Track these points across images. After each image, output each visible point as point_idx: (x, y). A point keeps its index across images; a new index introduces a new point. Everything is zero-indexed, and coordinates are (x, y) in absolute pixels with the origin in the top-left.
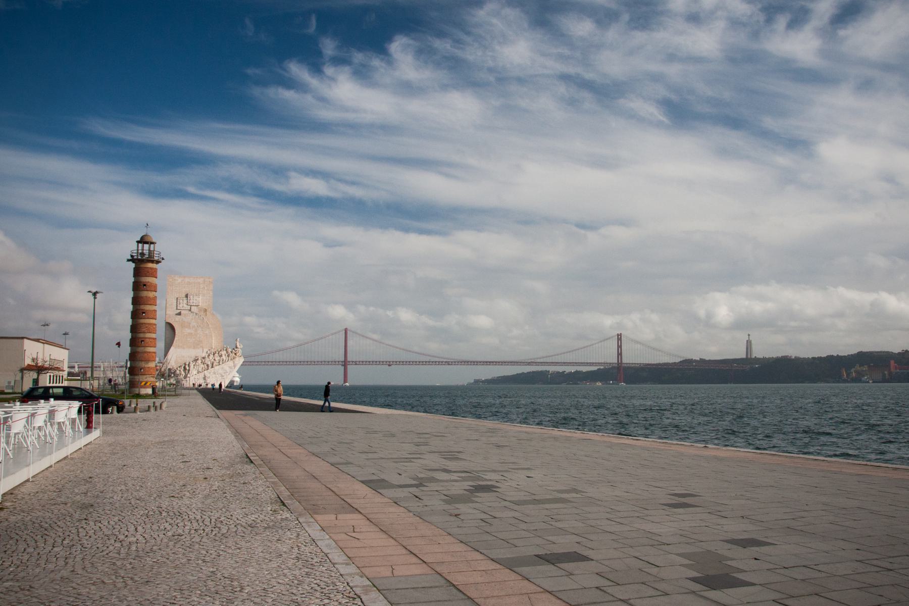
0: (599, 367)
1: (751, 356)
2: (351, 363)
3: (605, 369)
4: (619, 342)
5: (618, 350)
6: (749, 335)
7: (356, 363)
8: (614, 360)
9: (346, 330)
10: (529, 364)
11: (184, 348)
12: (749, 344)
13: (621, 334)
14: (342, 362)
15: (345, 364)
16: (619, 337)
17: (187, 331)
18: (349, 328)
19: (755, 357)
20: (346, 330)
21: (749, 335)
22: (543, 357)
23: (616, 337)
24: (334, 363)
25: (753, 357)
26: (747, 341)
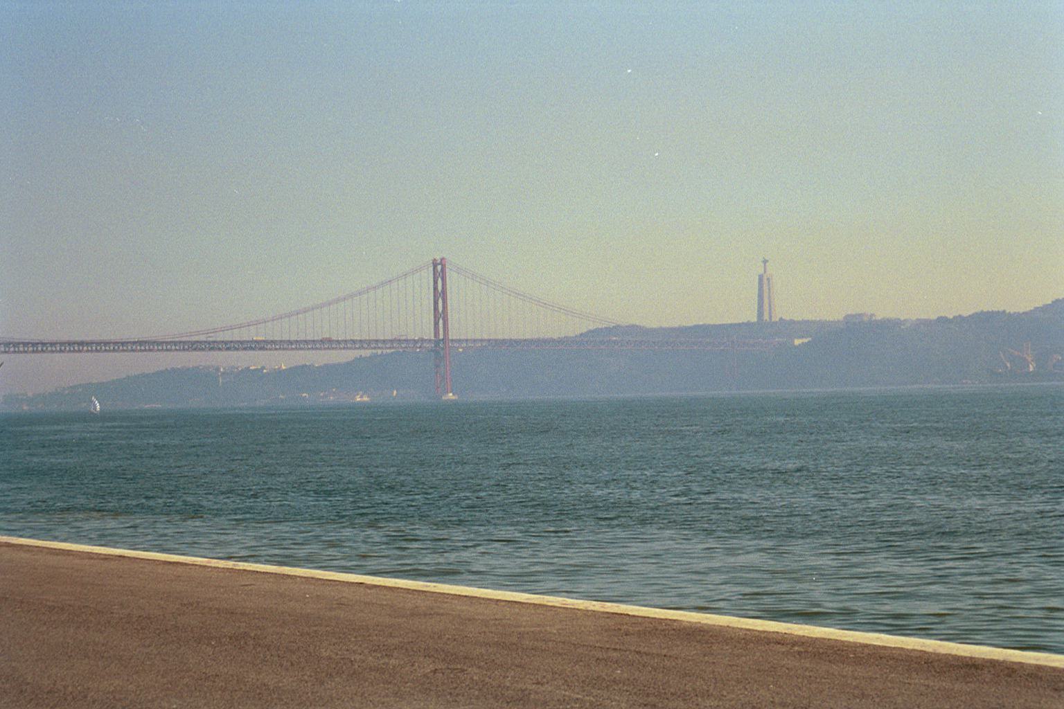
1: (770, 317)
5: (436, 303)
6: (765, 262)
8: (423, 328)
10: (194, 346)
12: (765, 281)
13: (442, 259)
16: (439, 269)
19: (781, 319)
21: (765, 262)
23: (431, 268)
25: (776, 319)
26: (761, 278)
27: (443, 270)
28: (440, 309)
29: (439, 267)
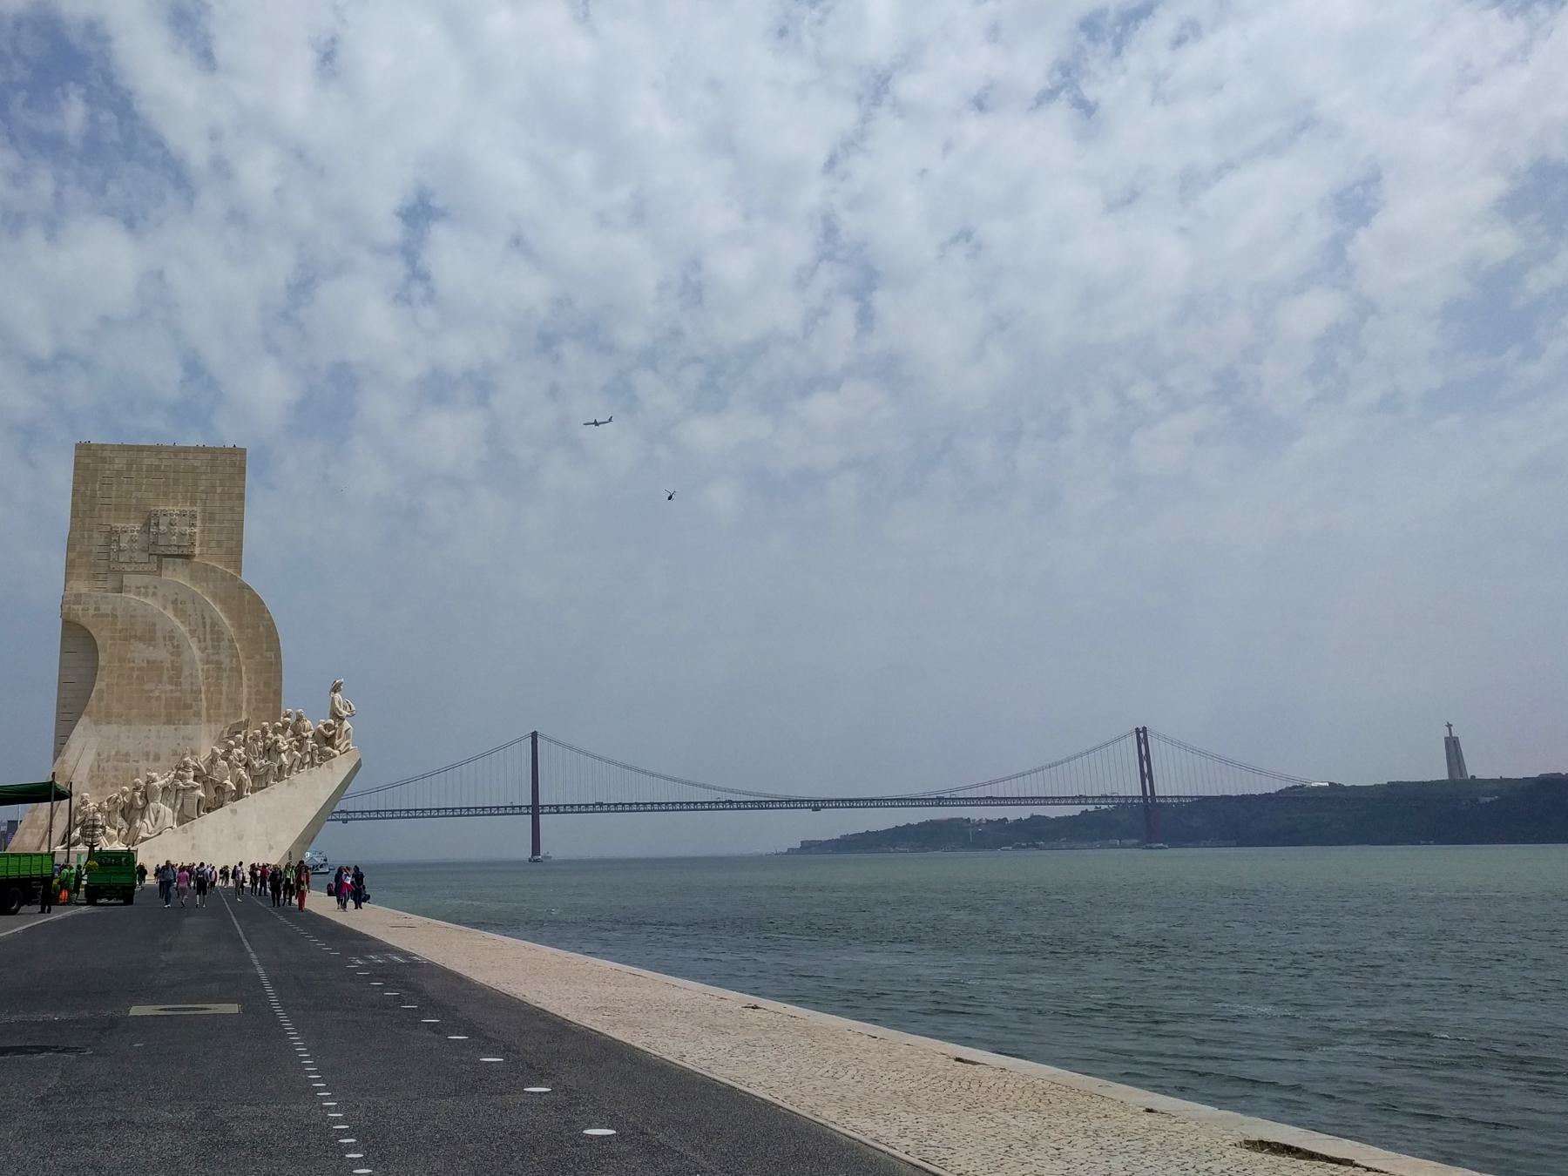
0: (1083, 808)
2: (546, 810)
3: (1097, 811)
4: (1143, 746)
7: (557, 809)
9: (534, 735)
11: (128, 722)
14: (528, 807)
15: (535, 810)
16: (1142, 735)
17: (141, 653)
18: (540, 732)
20: (534, 735)
22: (977, 786)
23: (1135, 736)
24: (512, 810)
27: (1145, 735)
28: (1146, 770)
29: (1142, 735)
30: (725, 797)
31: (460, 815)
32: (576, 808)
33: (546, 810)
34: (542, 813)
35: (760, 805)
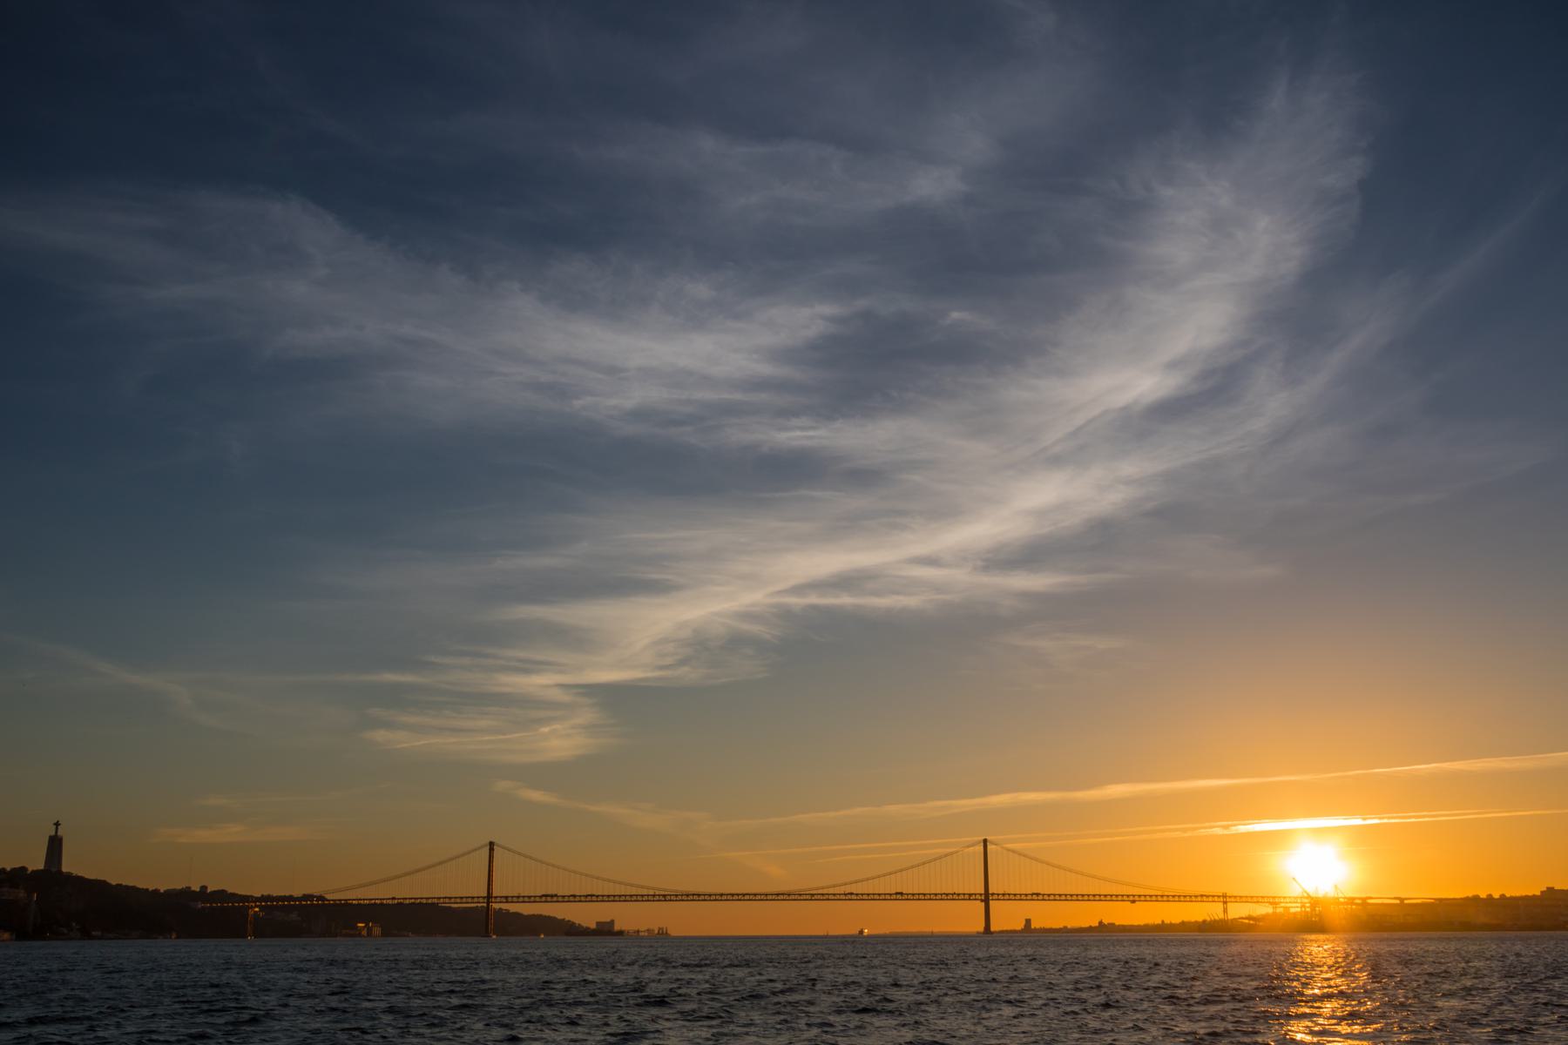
2: (995, 897)
9: (985, 841)
14: (981, 895)
15: (986, 898)
24: (970, 897)
30: (640, 892)
31: (930, 899)
32: (1018, 897)
33: (995, 897)
34: (993, 900)
35: (665, 898)
